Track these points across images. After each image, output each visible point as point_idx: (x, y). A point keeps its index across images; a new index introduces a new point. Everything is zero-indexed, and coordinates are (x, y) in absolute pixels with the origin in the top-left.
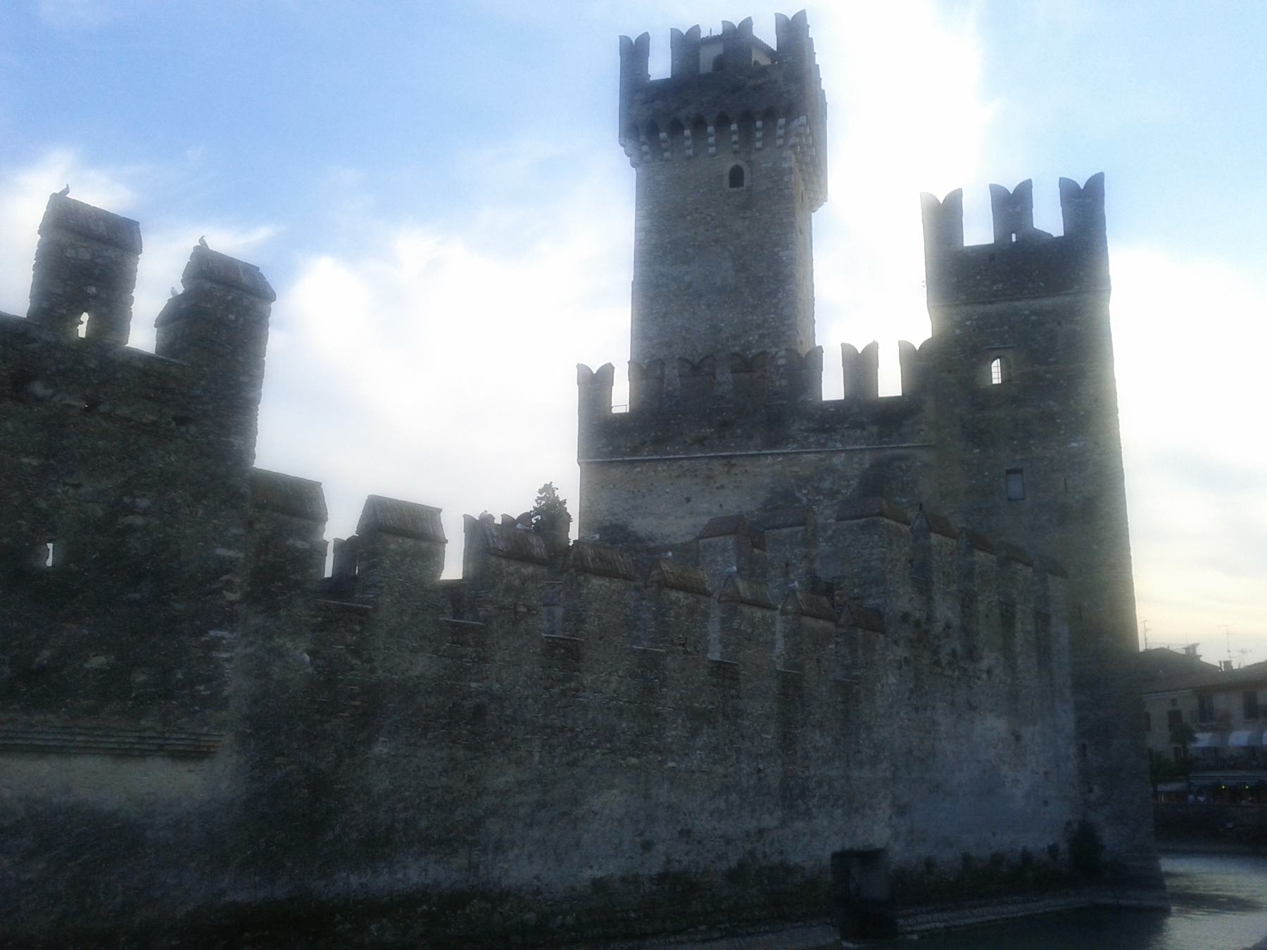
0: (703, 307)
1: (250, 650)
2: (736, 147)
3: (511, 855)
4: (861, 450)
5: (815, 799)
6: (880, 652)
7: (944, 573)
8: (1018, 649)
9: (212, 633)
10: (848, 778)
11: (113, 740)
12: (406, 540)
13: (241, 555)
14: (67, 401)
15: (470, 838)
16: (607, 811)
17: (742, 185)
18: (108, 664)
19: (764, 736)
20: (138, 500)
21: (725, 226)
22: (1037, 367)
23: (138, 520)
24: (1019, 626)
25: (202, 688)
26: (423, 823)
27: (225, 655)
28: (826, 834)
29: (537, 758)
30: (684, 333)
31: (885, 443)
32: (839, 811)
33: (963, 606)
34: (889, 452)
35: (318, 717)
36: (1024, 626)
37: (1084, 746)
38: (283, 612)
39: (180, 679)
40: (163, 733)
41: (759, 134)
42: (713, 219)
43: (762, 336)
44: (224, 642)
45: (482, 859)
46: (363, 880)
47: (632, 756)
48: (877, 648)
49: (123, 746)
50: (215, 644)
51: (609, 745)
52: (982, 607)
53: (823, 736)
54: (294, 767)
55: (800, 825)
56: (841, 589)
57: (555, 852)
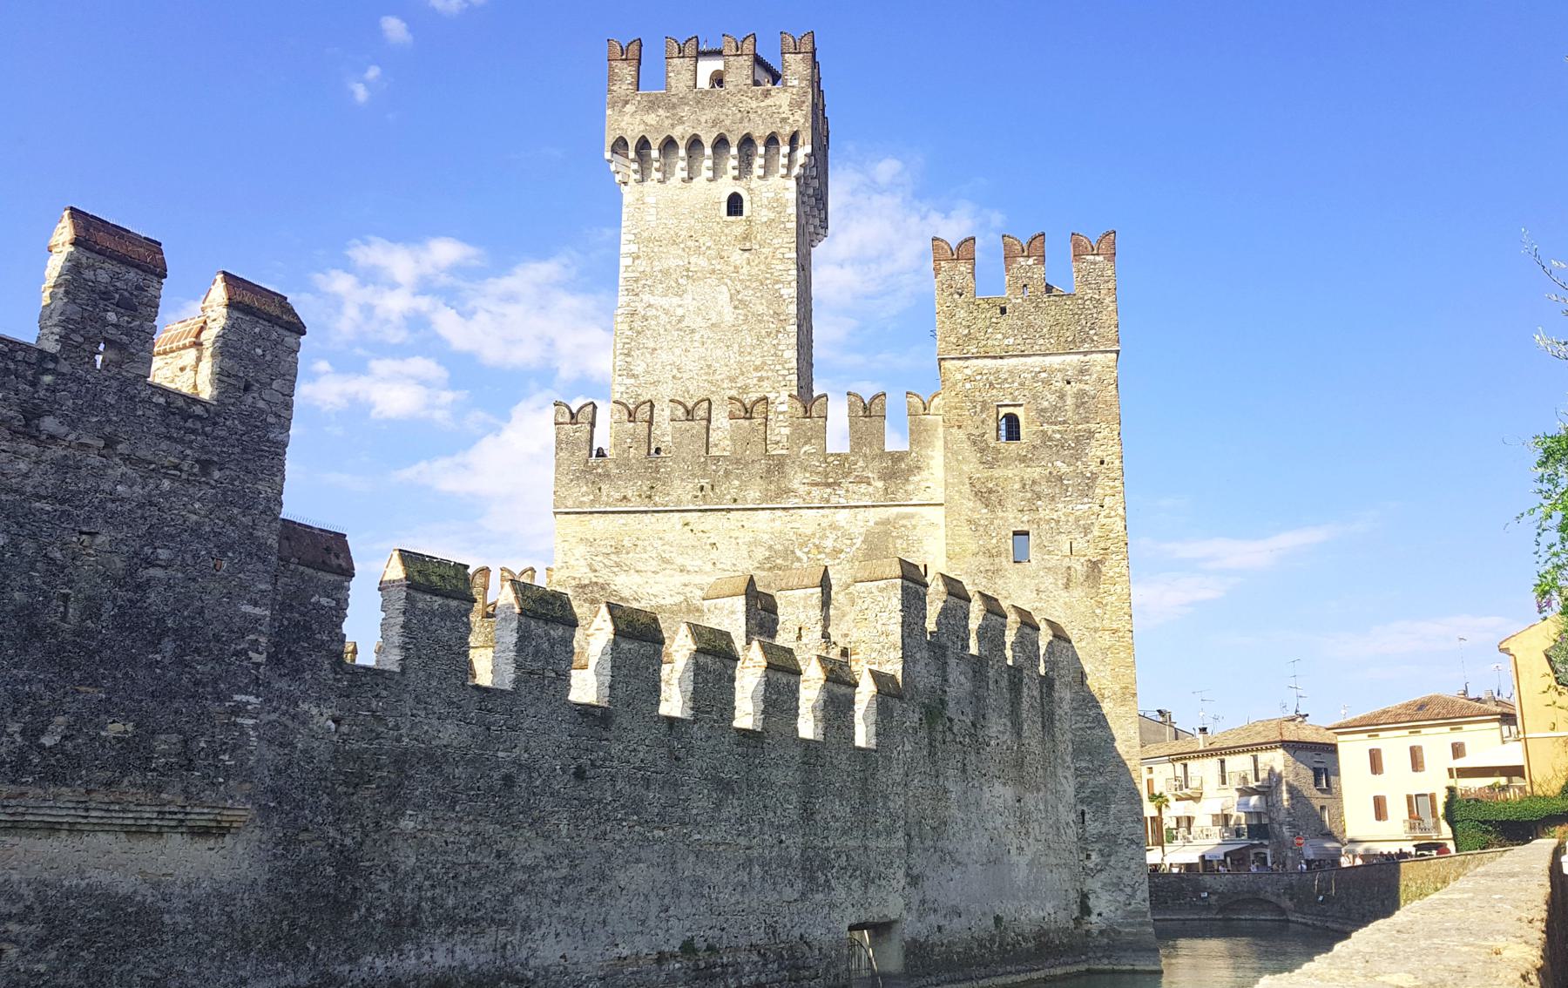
1: (274, 716)
3: (538, 934)
5: (834, 870)
9: (237, 697)
11: (130, 815)
12: (435, 598)
15: (496, 916)
16: (634, 887)
17: (741, 214)
18: (126, 732)
19: (786, 806)
20: (159, 551)
22: (1046, 426)
24: (1025, 690)
25: (227, 758)
26: (450, 902)
27: (251, 722)
28: (844, 905)
29: (564, 832)
30: (675, 371)
32: (856, 881)
33: (975, 672)
35: (340, 789)
36: (1030, 693)
37: (1083, 813)
38: (307, 675)
39: (203, 748)
40: (184, 807)
42: (709, 248)
43: (761, 379)
44: (249, 707)
45: (509, 939)
47: (658, 828)
49: (140, 822)
50: (239, 709)
51: (635, 818)
52: (991, 673)
54: (319, 843)
55: (820, 896)
56: (858, 654)
57: (582, 929)
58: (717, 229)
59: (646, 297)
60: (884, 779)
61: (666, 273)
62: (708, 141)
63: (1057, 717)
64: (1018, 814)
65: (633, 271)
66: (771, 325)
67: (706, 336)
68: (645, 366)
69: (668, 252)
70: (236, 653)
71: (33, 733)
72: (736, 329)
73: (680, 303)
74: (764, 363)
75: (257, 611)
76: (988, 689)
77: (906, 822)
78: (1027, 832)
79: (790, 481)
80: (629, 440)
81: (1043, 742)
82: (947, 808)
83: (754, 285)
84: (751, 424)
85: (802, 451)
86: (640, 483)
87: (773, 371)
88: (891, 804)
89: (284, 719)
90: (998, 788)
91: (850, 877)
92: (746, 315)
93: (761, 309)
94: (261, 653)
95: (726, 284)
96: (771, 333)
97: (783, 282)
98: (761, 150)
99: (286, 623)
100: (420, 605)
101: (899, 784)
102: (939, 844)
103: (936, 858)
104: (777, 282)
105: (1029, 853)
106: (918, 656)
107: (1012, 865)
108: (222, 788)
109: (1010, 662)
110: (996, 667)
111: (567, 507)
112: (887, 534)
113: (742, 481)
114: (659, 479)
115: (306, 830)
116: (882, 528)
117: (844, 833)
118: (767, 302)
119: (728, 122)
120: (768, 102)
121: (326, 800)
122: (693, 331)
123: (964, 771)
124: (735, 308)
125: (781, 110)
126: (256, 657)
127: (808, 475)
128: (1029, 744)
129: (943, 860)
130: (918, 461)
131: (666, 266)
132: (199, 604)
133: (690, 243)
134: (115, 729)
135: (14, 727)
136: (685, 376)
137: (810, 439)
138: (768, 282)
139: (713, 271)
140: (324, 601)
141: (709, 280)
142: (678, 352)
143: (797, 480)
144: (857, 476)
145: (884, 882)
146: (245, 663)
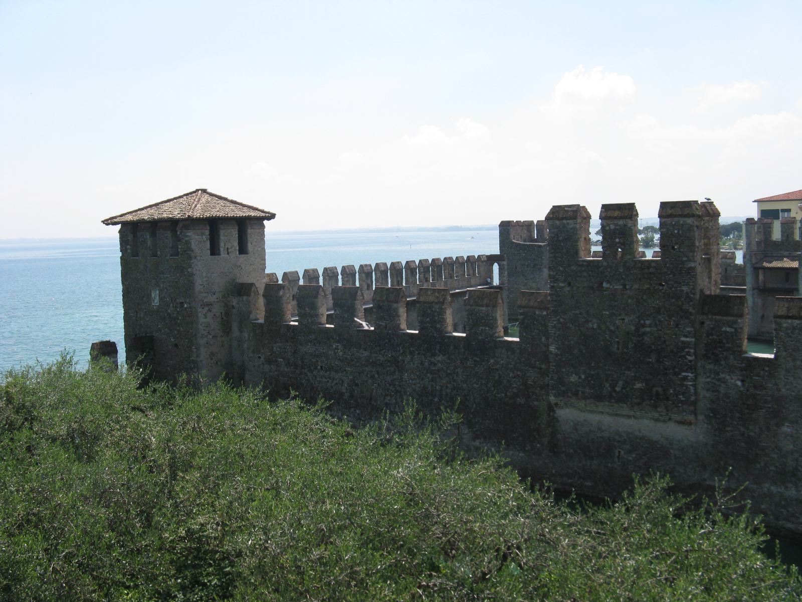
1: (708, 380)
9: (683, 374)
12: (794, 321)
13: (693, 340)
14: (616, 287)
23: (648, 329)
25: (681, 397)
46: (779, 490)
50: (685, 379)
70: (681, 357)
71: (613, 386)
75: (688, 339)
89: (713, 381)
94: (692, 356)
99: (709, 341)
100: (785, 325)
108: (681, 408)
115: (729, 426)
121: (738, 415)
126: (689, 358)
132: (663, 339)
134: (638, 385)
135: (607, 385)
140: (728, 329)
146: (685, 360)
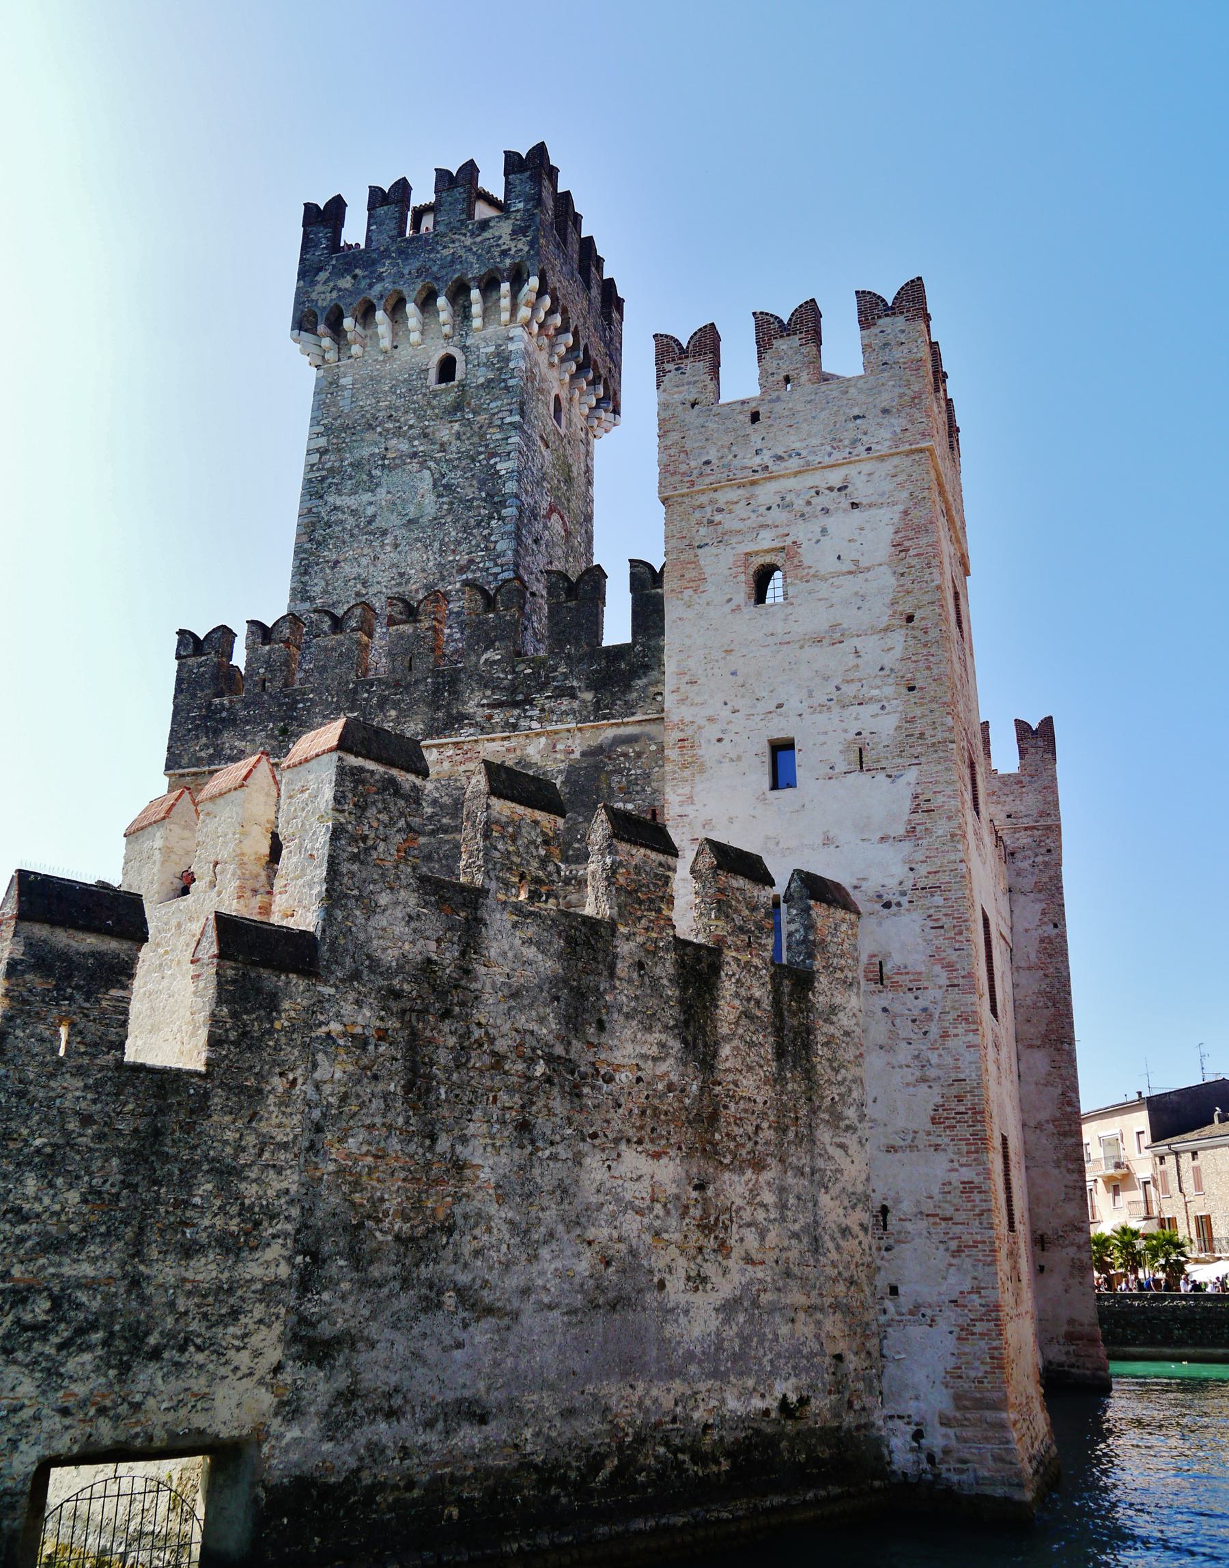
0: (388, 548)
2: (447, 329)
4: (568, 731)
6: (293, 1014)
7: (522, 877)
8: (724, 1030)
10: (136, 1282)
21: (426, 436)
24: (727, 987)
28: (26, 1414)
30: (359, 586)
31: (605, 717)
32: (87, 1357)
33: (571, 941)
34: (610, 733)
41: (476, 309)
42: (411, 427)
48: (286, 1005)
52: (624, 948)
53: (51, 1185)
58: (423, 402)
59: (331, 499)
60: (230, 1135)
61: (357, 465)
62: (412, 292)
63: (821, 1039)
64: (696, 1212)
65: (319, 470)
66: (483, 511)
67: (399, 537)
68: (323, 583)
69: (362, 440)
72: (437, 522)
73: (373, 499)
74: (471, 561)
76: (612, 975)
77: (304, 1227)
78: (723, 1248)
79: (465, 703)
80: (262, 671)
81: (778, 1080)
82: (458, 1199)
83: (464, 462)
84: (416, 628)
85: (482, 661)
86: (271, 725)
87: (481, 570)
88: (250, 1191)
90: (633, 1160)
91: (60, 1347)
92: (451, 503)
93: (470, 493)
95: (429, 468)
96: (482, 521)
97: (499, 455)
98: (475, 294)
101: (284, 1146)
102: (424, 1272)
103: (405, 1301)
104: (494, 455)
105: (725, 1287)
106: (384, 899)
107: (672, 1310)
109: (785, 961)
110: (640, 939)
111: (181, 767)
112: (598, 768)
113: (400, 711)
114: (295, 718)
116: (591, 760)
117: (52, 1246)
118: (479, 482)
119: (435, 269)
120: (486, 235)
122: (384, 533)
123: (524, 1127)
124: (439, 496)
125: (500, 242)
127: (488, 693)
128: (735, 1083)
129: (431, 1305)
130: (644, 657)
131: (357, 456)
133: (390, 425)
136: (372, 591)
137: (493, 642)
138: (482, 457)
139: (414, 455)
141: (409, 467)
142: (364, 561)
143: (474, 703)
144: (556, 687)
145: (200, 1358)
